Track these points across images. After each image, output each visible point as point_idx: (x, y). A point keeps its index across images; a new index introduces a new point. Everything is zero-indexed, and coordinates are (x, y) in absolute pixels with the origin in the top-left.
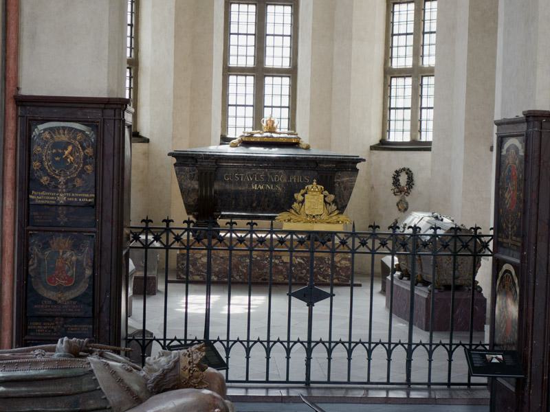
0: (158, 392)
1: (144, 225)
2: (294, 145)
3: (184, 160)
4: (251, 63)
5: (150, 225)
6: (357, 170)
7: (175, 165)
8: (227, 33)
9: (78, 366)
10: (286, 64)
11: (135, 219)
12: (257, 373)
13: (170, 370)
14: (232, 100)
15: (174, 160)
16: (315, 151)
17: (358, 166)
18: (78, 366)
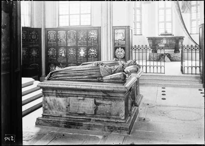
0: (128, 66)
1: (135, 46)
2: (171, 35)
3: (149, 39)
4: (163, 20)
5: (136, 46)
6: (183, 39)
7: (148, 39)
8: (159, 15)
9: (117, 62)
10: (170, 20)
11: (133, 46)
12: (155, 71)
13: (130, 63)
14: (160, 28)
15: (148, 39)
16: (175, 36)
17: (184, 38)
18: (117, 62)
